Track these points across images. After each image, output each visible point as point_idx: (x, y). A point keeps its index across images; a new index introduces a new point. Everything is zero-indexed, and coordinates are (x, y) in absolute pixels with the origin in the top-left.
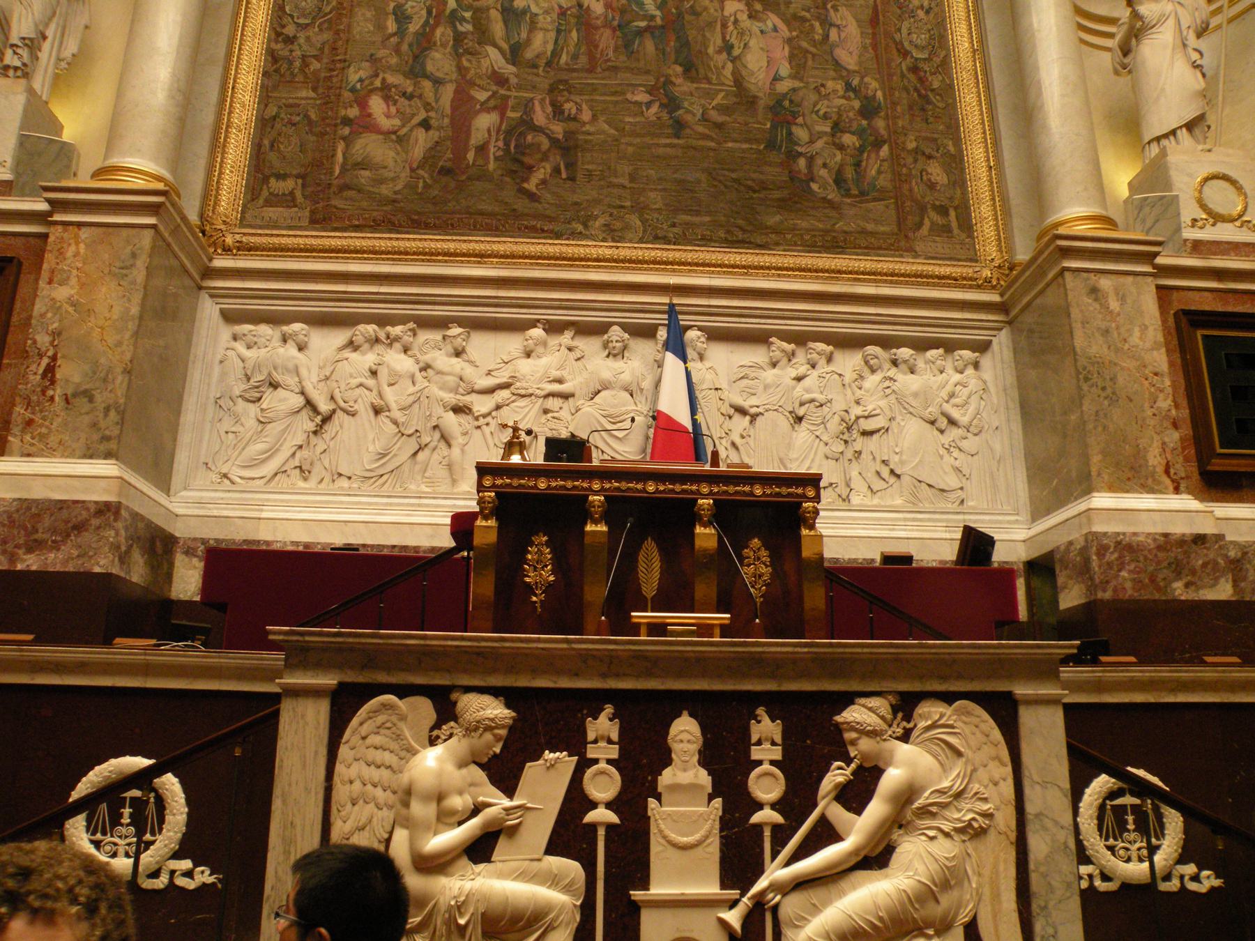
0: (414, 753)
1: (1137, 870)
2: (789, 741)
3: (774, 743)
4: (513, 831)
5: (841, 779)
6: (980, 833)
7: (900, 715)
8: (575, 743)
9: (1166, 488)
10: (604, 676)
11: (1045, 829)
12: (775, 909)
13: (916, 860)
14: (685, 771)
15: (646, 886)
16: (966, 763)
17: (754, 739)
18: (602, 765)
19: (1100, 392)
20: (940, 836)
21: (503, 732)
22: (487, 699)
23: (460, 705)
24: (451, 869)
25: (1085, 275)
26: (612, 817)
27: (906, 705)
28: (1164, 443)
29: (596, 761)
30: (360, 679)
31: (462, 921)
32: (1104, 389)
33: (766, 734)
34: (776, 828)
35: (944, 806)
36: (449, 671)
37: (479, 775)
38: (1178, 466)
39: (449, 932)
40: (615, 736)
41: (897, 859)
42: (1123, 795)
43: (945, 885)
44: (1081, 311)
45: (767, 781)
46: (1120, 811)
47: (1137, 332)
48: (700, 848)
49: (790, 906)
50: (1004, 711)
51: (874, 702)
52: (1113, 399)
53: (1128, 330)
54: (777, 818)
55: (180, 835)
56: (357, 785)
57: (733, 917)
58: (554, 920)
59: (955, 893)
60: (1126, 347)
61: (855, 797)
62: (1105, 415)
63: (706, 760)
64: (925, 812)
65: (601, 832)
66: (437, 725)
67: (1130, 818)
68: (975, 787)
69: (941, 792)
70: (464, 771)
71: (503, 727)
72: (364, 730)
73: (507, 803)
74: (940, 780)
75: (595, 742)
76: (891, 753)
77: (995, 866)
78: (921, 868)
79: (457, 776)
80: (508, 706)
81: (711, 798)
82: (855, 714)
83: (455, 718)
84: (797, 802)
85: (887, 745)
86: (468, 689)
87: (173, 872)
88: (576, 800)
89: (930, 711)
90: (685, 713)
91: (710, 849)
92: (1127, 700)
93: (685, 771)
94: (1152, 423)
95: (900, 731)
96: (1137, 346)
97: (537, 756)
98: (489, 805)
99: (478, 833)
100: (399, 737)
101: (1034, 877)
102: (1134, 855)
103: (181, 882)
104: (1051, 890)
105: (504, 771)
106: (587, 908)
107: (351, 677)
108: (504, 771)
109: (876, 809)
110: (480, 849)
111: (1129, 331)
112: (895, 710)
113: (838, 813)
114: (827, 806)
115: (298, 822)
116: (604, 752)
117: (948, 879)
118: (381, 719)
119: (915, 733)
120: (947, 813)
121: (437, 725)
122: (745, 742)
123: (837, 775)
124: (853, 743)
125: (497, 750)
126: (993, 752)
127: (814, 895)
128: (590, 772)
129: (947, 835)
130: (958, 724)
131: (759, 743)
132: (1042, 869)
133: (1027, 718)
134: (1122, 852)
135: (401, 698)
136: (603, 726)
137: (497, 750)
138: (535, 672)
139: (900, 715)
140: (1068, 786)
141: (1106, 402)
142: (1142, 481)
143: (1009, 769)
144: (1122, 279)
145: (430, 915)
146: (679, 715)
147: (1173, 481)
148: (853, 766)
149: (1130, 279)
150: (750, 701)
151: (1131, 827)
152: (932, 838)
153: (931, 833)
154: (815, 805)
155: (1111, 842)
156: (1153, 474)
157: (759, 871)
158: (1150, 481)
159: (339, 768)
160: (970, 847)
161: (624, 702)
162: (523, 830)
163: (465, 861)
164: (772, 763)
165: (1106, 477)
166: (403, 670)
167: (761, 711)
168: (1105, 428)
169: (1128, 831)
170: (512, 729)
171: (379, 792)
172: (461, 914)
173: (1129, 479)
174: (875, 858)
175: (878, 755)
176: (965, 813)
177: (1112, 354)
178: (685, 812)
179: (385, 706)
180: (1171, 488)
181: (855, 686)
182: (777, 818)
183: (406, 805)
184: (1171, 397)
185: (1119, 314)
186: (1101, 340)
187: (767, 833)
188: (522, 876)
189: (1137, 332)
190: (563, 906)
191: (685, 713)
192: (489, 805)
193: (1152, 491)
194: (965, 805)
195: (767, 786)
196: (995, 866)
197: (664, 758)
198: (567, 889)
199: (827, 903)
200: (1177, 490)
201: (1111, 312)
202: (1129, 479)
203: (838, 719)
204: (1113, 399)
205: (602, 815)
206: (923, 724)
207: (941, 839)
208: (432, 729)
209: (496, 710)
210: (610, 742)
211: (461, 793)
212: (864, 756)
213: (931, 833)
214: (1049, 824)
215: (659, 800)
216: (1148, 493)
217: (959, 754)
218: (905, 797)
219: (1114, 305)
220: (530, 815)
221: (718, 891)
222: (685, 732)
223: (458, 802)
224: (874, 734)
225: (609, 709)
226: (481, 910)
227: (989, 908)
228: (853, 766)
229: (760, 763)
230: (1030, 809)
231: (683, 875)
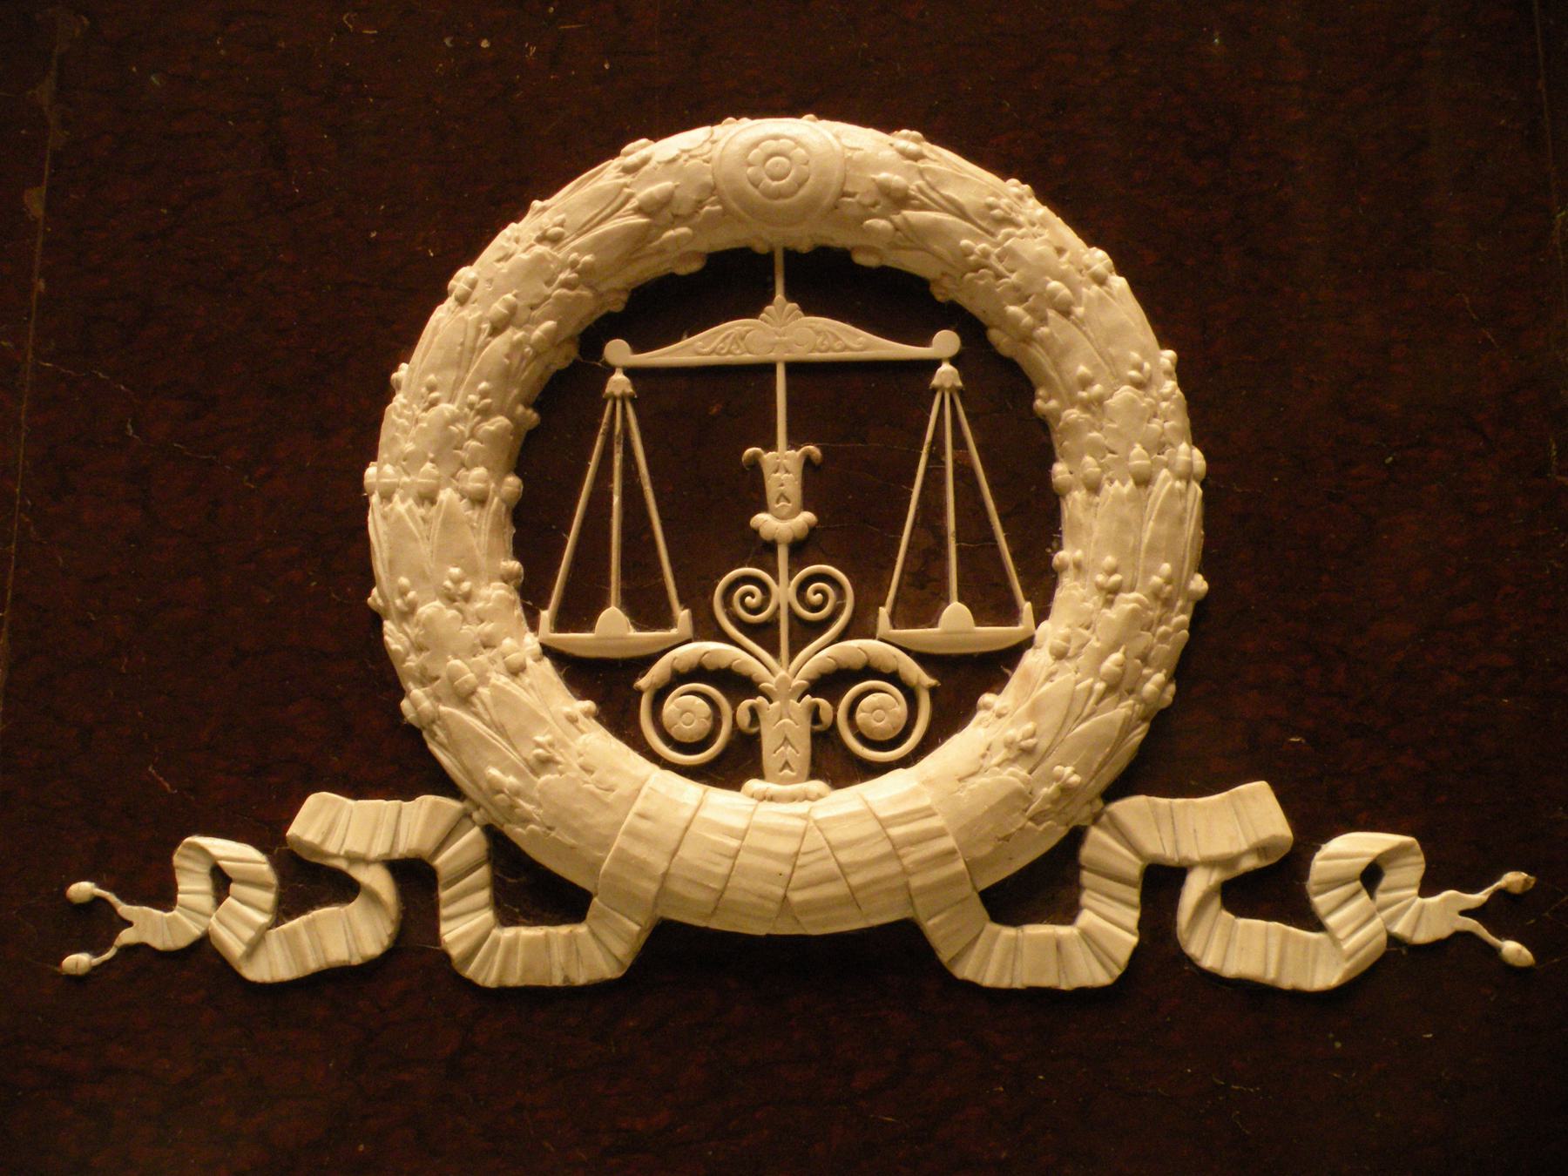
1: (778, 838)
42: (751, 303)
67: (782, 466)
102: (784, 727)
134: (687, 710)
151: (781, 521)
169: (763, 551)
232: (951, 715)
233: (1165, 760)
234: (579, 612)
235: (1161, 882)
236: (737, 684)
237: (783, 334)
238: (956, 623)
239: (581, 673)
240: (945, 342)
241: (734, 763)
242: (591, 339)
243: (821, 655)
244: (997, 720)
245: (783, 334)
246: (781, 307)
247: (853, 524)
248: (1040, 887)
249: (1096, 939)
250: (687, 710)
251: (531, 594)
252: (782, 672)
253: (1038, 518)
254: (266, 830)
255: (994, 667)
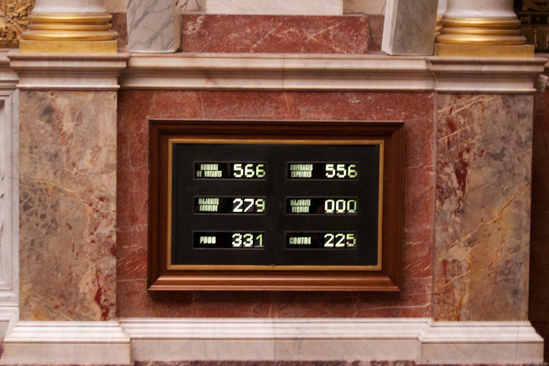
9: (94, 314)
19: (39, 220)
25: (41, 94)
28: (98, 271)
32: (43, 217)
38: (109, 293)
44: (32, 135)
47: (88, 155)
52: (52, 227)
53: (79, 153)
60: (75, 170)
62: (41, 244)
94: (89, 250)
96: (85, 170)
111: (81, 154)
141: (44, 231)
142: (70, 308)
144: (81, 97)
147: (102, 307)
149: (91, 96)
156: (82, 302)
158: (78, 308)
165: (34, 305)
168: (39, 256)
173: (57, 307)
177: (58, 180)
180: (99, 315)
184: (114, 222)
185: (71, 136)
186: (47, 165)
189: (88, 155)
193: (78, 318)
200: (105, 317)
201: (63, 134)
202: (57, 307)
204: (52, 227)
216: (75, 320)
219: (68, 125)
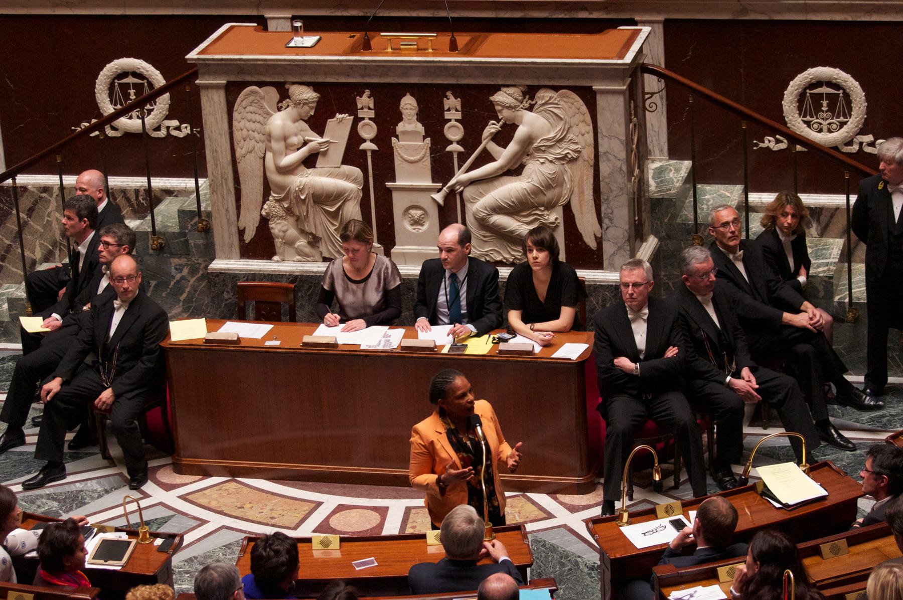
0: (271, 115)
2: (466, 109)
3: (457, 110)
4: (325, 154)
5: (493, 130)
6: (573, 160)
7: (527, 97)
8: (351, 109)
10: (363, 76)
11: (609, 160)
12: (461, 193)
13: (536, 172)
14: (410, 124)
15: (393, 180)
16: (565, 124)
17: (446, 108)
18: (367, 121)
20: (547, 163)
21: (314, 105)
22: (303, 88)
23: (290, 91)
24: (296, 172)
26: (374, 147)
27: (530, 92)
29: (363, 119)
30: (237, 80)
31: (303, 197)
33: (453, 106)
34: (459, 153)
35: (551, 147)
36: (281, 74)
37: (305, 126)
39: (297, 202)
40: (372, 106)
41: (526, 171)
42: (821, 87)
43: (549, 187)
45: (453, 130)
46: (817, 98)
48: (420, 164)
49: (469, 192)
50: (589, 97)
51: (511, 90)
54: (461, 149)
55: (167, 106)
56: (245, 131)
57: (439, 197)
58: (348, 196)
59: (557, 191)
61: (504, 137)
63: (422, 117)
64: (538, 149)
65: (369, 154)
66: (280, 101)
67: (825, 103)
68: (570, 136)
69: (548, 140)
70: (297, 124)
71: (313, 102)
72: (244, 104)
73: (320, 140)
74: (549, 132)
75: (362, 109)
76: (522, 117)
77: (582, 177)
78: (535, 178)
79: (292, 127)
80: (315, 91)
81: (424, 138)
82: (500, 97)
83: (289, 98)
84: (471, 140)
85: (519, 113)
86: (294, 83)
87: (168, 128)
88: (354, 139)
89: (544, 95)
90: (408, 94)
91: (426, 163)
92: (828, 19)
93: (410, 124)
95: (527, 105)
97: (333, 116)
98: (311, 141)
99: (307, 155)
100: (262, 107)
101: (602, 184)
102: (825, 128)
103: (175, 133)
104: (611, 191)
105: (317, 124)
106: (365, 189)
107: (233, 78)
108: (317, 124)
109: (512, 147)
110: (310, 161)
112: (524, 94)
113: (493, 147)
114: (487, 143)
115: (218, 149)
116: (367, 114)
117: (553, 183)
118: (251, 98)
119: (536, 107)
120: (552, 150)
121: (280, 101)
122: (441, 110)
123: (492, 128)
124: (500, 111)
125: (312, 114)
126: (582, 118)
127: (481, 188)
128: (360, 124)
129: (551, 162)
130: (562, 103)
131: (449, 110)
132: (607, 180)
133: (601, 101)
134: (816, 126)
135: (260, 87)
136: (365, 101)
137: (312, 114)
138: (326, 74)
139: (527, 97)
140: (624, 138)
143: (591, 127)
145: (288, 193)
146: (405, 95)
148: (501, 123)
150: (445, 88)
152: (542, 163)
153: (542, 161)
154: (481, 143)
155: (808, 118)
157: (452, 175)
159: (235, 123)
160: (567, 167)
161: (377, 90)
162: (330, 152)
163: (302, 167)
164: (456, 120)
166: (258, 74)
167: (449, 94)
169: (823, 111)
170: (318, 103)
171: (256, 134)
172: (302, 194)
174: (514, 170)
175: (514, 118)
176: (559, 151)
178: (411, 144)
179: (253, 92)
181: (500, 82)
182: (461, 149)
183: (270, 141)
187: (455, 156)
188: (330, 175)
190: (351, 191)
191: (408, 94)
192: (311, 141)
194: (564, 145)
195: (454, 132)
196: (582, 177)
197: (398, 117)
198: (354, 181)
199: (487, 192)
203: (492, 98)
205: (369, 146)
206: (540, 102)
207: (547, 164)
208: (278, 103)
209: (308, 94)
210: (369, 109)
211: (296, 135)
212: (506, 119)
213: (542, 161)
214: (612, 158)
215: (398, 138)
217: (561, 119)
218: (528, 141)
220: (332, 146)
221: (431, 184)
222: (409, 104)
223: (295, 140)
224: (510, 107)
225: (367, 92)
226: (311, 192)
227: (577, 198)
228: (501, 123)
229: (450, 120)
230: (600, 149)
231: (411, 176)
232: (841, 127)
233: (862, 132)
234: (805, 116)
235: (861, 144)
236: (820, 124)
237: (825, 90)
238: (842, 119)
239: (805, 122)
240: (841, 91)
241: (820, 131)
242: (805, 89)
243: (829, 121)
244: (845, 128)
245: (825, 90)
246: (824, 87)
247: (832, 108)
248: (850, 143)
249: (855, 148)
250: (816, 126)
251: (800, 114)
252: (825, 123)
253: (850, 109)
254: (774, 137)
255: (846, 123)
